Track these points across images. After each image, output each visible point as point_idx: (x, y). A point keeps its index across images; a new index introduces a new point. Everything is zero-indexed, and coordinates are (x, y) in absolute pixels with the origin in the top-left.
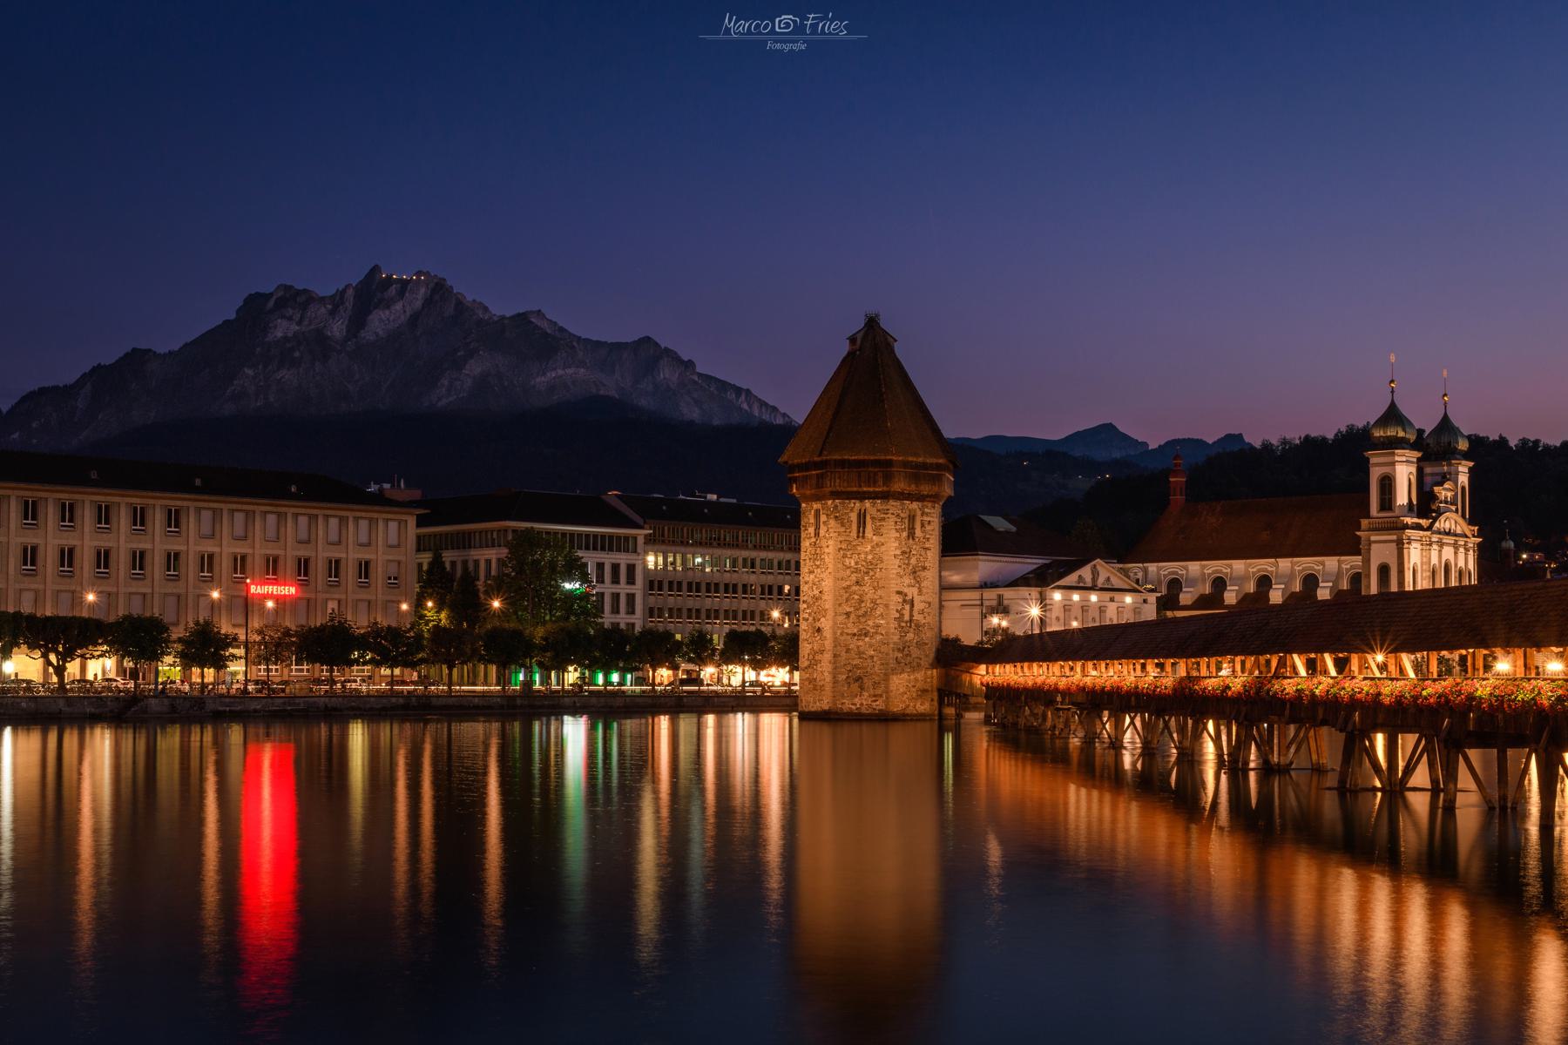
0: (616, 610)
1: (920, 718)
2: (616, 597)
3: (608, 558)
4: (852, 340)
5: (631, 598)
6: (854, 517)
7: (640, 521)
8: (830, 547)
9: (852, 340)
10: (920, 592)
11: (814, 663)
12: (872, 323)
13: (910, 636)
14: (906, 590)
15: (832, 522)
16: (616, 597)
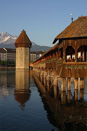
1: (28, 69)
8: (19, 52)
11: (17, 63)
12: (24, 30)
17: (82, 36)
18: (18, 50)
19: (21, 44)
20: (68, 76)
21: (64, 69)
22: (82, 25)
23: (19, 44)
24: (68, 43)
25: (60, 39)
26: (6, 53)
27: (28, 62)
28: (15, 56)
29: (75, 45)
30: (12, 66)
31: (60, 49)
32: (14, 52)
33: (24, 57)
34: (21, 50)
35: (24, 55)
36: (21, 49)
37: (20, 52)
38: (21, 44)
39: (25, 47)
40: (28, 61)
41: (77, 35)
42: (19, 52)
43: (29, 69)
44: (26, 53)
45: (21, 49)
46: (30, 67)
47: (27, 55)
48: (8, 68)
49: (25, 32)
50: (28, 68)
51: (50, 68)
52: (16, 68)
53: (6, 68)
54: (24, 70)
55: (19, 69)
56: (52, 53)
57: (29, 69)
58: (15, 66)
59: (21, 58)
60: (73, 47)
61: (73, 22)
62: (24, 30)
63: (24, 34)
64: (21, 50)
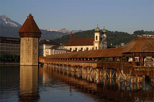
1: (36, 65)
4: (28, 17)
6: (28, 40)
8: (25, 44)
9: (28, 17)
11: (22, 58)
12: (30, 15)
17: (145, 51)
18: (23, 41)
19: (28, 33)
21: (133, 70)
23: (26, 33)
27: (37, 57)
28: (18, 48)
30: (13, 61)
32: (19, 42)
33: (32, 50)
34: (29, 41)
35: (32, 47)
37: (27, 43)
38: (28, 33)
39: (33, 37)
40: (37, 55)
42: (25, 44)
43: (39, 65)
46: (39, 63)
47: (36, 47)
48: (6, 63)
50: (37, 64)
52: (21, 64)
53: (3, 64)
54: (31, 67)
55: (25, 65)
57: (39, 65)
58: (19, 60)
59: (28, 52)
62: (30, 15)
63: (30, 21)
64: (29, 41)
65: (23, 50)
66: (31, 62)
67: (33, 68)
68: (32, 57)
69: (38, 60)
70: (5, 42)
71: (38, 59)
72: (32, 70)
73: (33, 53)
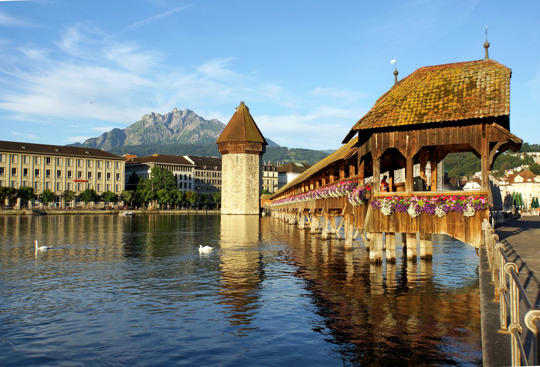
0: (185, 187)
2: (185, 184)
3: (183, 173)
5: (190, 184)
7: (193, 163)
10: (254, 180)
11: (225, 200)
13: (251, 192)
14: (251, 179)
15: (229, 160)
16: (185, 184)
17: (426, 120)
20: (388, 229)
22: (426, 92)
23: (231, 143)
24: (387, 142)
25: (363, 134)
26: (193, 169)
27: (258, 196)
28: (217, 179)
29: (405, 146)
31: (363, 158)
33: (244, 181)
34: (237, 161)
35: (244, 174)
36: (237, 157)
38: (236, 143)
39: (247, 152)
40: (257, 192)
41: (412, 119)
43: (260, 215)
44: (250, 169)
45: (237, 157)
46: (261, 210)
47: (253, 174)
49: (247, 109)
50: (258, 212)
51: (329, 209)
56: (336, 168)
60: (402, 151)
61: (398, 83)
62: (243, 103)
64: (237, 161)
65: (225, 182)
66: (244, 207)
67: (246, 220)
68: (245, 196)
69: (258, 203)
70: (205, 167)
71: (260, 200)
72: (246, 225)
73: (248, 187)
